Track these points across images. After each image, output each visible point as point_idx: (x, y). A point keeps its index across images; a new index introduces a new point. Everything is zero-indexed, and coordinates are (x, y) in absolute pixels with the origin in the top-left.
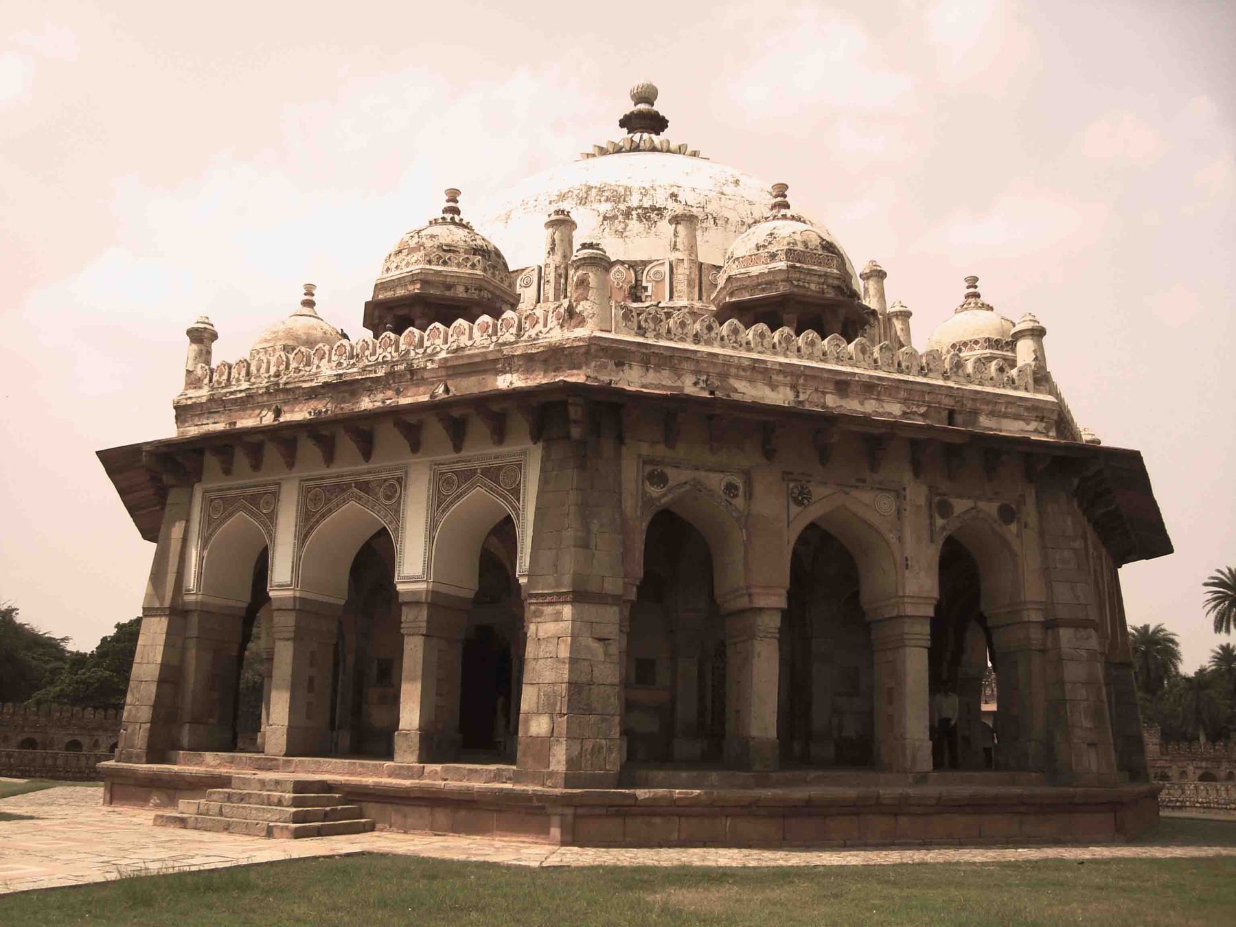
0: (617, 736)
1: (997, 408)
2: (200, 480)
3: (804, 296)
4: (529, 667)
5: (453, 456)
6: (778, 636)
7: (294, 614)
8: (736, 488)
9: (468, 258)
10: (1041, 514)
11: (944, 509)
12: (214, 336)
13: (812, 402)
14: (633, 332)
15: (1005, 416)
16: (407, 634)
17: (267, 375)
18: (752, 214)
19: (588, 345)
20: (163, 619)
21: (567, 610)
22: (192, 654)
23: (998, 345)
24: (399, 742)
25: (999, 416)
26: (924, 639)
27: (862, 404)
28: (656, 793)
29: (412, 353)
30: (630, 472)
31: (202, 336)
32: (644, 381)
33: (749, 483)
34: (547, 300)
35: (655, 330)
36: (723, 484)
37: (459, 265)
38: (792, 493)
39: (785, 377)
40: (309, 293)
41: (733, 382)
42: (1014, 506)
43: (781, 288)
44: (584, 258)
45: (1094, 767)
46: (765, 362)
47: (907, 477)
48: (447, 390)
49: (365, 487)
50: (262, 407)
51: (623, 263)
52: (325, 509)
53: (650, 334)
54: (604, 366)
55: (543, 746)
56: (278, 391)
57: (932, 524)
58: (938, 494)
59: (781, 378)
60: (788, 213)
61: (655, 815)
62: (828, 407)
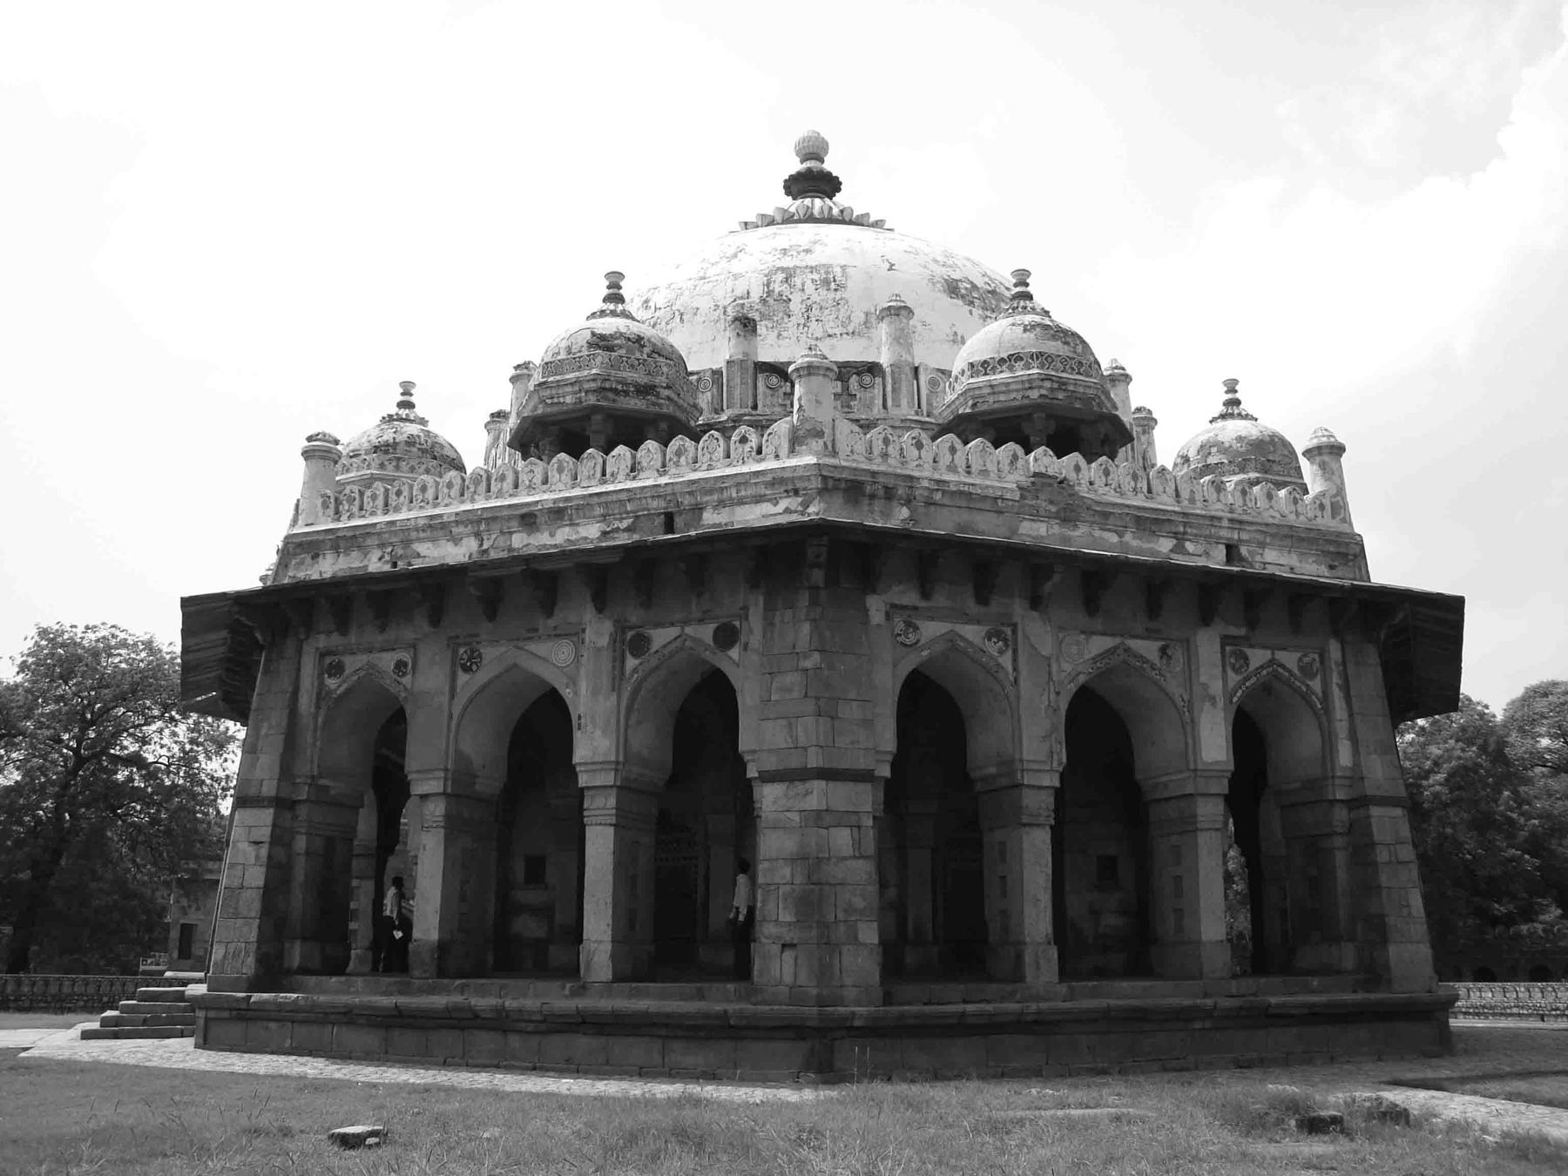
1: (725, 494)
8: (405, 665)
10: (769, 624)
11: (639, 645)
13: (496, 548)
15: (741, 502)
23: (986, 369)
25: (732, 505)
27: (552, 535)
32: (336, 568)
35: (348, 511)
39: (466, 526)
41: (422, 548)
46: (440, 516)
47: (589, 614)
53: (344, 517)
54: (302, 563)
58: (631, 628)
59: (461, 529)
62: (514, 550)
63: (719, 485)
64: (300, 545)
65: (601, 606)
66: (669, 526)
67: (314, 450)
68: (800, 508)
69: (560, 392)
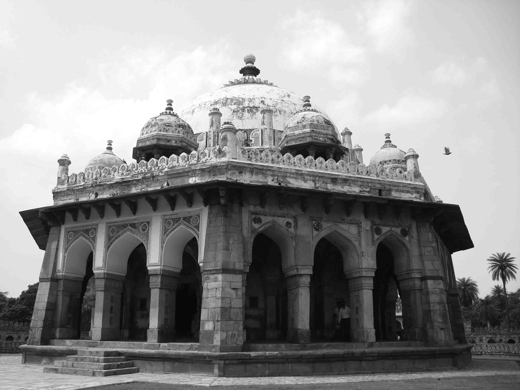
0: (242, 329)
1: (399, 188)
2: (63, 224)
3: (318, 143)
4: (204, 301)
5: (171, 212)
6: (309, 286)
7: (104, 280)
8: (290, 224)
9: (176, 129)
11: (378, 231)
12: (69, 163)
13: (321, 187)
14: (246, 159)
15: (403, 191)
16: (152, 288)
17: (92, 179)
18: (295, 109)
19: (228, 165)
20: (48, 283)
21: (220, 277)
22: (60, 298)
24: (149, 334)
26: (371, 286)
27: (343, 188)
28: (259, 354)
29: (153, 169)
30: (246, 218)
31: (64, 163)
33: (296, 221)
34: (210, 146)
35: (255, 158)
36: (285, 222)
37: (173, 132)
38: (314, 225)
39: (310, 177)
40: (110, 144)
41: (289, 179)
42: (407, 229)
43: (308, 140)
44: (225, 128)
45: (443, 339)
46: (302, 171)
47: (362, 218)
48: (168, 184)
49: (133, 226)
50: (90, 193)
51: (242, 130)
52: (117, 235)
53: (253, 160)
54: (233, 174)
55: (210, 335)
56: (97, 186)
57: (373, 237)
58: (376, 225)
59: (308, 177)
60: (311, 108)
61: (258, 363)
62: (328, 189)
63: (398, 185)
64: (235, 166)
65: (366, 217)
66: (380, 194)
67: (233, 129)
68: (419, 198)
69: (319, 135)
